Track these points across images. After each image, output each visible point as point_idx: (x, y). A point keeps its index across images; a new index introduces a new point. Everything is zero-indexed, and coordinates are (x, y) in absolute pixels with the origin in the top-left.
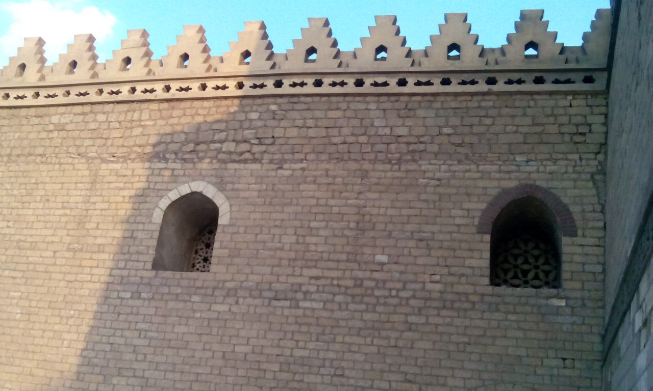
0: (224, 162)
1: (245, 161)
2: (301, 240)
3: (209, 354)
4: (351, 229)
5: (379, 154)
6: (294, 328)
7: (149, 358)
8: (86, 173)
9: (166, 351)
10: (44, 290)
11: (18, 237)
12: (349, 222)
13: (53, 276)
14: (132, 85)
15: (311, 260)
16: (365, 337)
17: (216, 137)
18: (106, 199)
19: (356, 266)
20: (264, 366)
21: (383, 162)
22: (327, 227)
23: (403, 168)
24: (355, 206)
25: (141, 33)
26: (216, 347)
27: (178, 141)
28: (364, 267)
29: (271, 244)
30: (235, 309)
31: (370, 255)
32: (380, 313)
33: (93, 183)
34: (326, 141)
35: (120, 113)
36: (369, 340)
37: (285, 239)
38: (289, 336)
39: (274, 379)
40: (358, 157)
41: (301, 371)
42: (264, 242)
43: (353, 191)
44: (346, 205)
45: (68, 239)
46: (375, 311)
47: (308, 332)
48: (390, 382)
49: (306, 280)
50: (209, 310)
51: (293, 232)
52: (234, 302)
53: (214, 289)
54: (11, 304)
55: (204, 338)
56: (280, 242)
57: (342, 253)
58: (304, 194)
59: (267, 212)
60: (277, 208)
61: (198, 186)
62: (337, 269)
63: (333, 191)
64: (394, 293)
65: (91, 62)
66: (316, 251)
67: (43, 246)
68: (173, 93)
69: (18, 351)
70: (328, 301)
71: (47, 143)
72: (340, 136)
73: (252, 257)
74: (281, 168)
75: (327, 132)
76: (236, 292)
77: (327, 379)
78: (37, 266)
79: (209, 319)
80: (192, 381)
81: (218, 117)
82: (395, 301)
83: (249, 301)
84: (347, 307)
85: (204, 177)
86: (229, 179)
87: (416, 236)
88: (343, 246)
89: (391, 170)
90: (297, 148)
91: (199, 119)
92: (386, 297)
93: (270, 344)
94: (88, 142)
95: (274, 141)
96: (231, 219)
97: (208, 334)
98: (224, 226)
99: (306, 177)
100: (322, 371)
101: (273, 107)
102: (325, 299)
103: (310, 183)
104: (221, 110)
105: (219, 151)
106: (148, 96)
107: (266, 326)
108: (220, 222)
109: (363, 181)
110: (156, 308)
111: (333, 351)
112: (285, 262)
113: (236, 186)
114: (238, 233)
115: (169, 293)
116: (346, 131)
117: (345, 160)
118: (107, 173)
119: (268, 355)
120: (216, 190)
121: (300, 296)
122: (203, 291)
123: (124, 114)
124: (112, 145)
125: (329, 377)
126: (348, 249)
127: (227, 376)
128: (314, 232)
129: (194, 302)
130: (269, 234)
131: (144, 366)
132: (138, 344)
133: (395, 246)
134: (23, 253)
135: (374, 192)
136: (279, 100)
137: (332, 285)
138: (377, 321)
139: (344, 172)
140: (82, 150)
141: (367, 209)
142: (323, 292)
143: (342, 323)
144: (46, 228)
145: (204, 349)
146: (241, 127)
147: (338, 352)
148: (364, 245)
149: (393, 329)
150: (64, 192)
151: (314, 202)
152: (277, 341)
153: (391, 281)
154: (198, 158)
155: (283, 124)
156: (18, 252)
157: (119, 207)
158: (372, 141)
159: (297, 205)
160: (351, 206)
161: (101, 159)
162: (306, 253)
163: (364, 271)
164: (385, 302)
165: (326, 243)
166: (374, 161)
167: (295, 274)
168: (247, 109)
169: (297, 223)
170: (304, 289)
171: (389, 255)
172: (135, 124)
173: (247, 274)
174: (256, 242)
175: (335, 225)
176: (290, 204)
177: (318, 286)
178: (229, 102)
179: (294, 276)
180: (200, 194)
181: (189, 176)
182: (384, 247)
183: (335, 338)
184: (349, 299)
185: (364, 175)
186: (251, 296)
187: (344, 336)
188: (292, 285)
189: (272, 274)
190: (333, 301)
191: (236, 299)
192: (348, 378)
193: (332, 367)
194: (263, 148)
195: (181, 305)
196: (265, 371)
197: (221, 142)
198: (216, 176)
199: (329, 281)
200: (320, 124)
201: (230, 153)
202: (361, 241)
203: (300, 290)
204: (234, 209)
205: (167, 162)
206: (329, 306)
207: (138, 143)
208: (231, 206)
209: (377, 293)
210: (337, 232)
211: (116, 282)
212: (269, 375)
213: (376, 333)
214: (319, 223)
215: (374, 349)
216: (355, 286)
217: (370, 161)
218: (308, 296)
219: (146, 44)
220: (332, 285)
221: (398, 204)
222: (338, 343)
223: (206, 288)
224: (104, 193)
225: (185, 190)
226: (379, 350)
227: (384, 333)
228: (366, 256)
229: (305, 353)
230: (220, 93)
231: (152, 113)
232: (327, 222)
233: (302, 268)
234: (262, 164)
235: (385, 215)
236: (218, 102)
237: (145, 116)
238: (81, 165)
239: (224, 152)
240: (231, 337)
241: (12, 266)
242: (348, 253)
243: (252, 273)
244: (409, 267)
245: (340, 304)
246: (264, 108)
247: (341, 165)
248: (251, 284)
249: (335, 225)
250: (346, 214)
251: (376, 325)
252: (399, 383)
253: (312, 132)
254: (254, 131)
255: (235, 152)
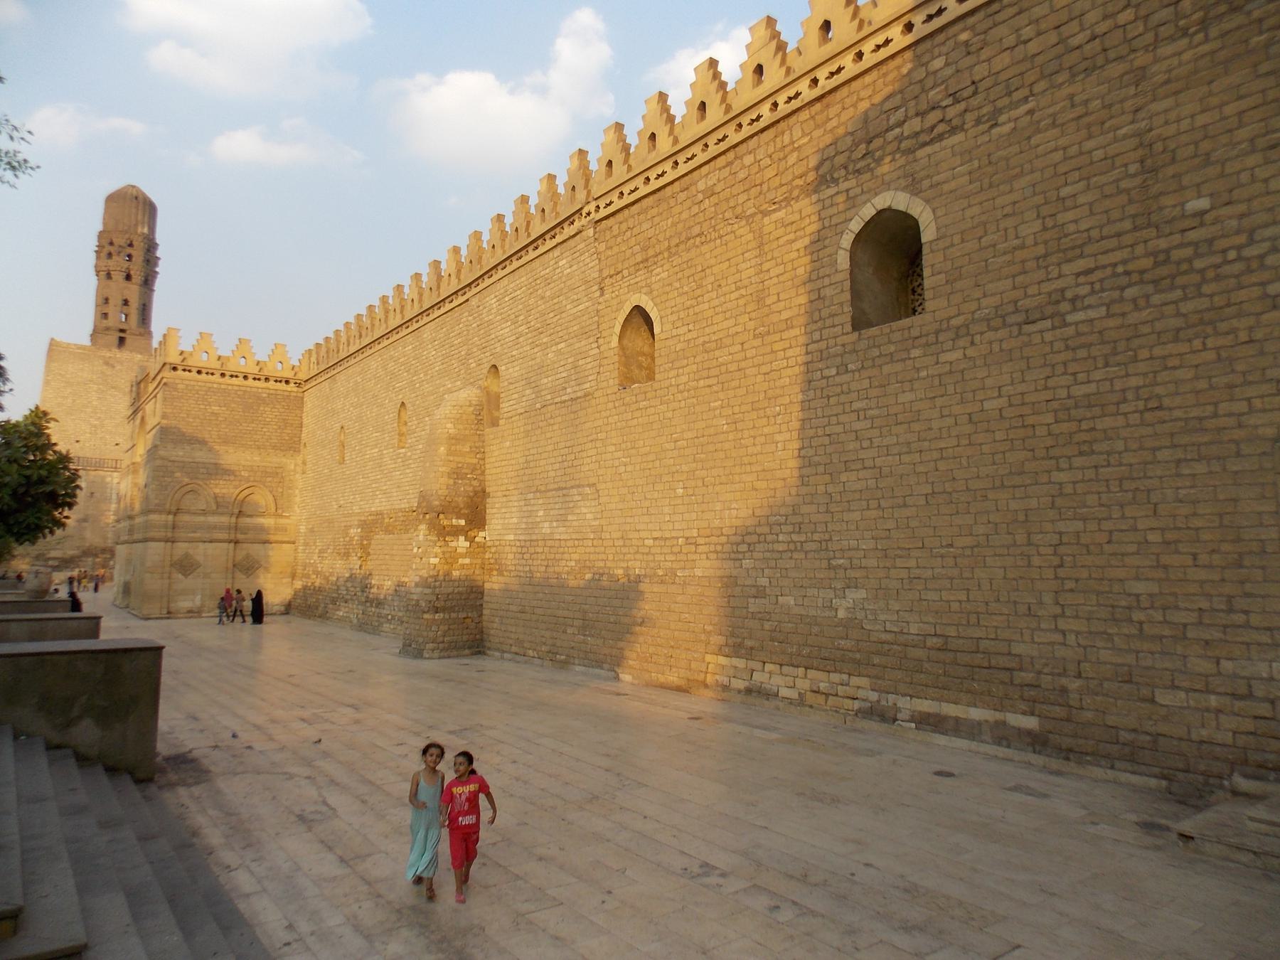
0: (911, 151)
1: (940, 137)
2: (1049, 222)
3: (950, 421)
4: (1134, 176)
5: (1162, 29)
6: (1069, 355)
7: (876, 442)
8: (750, 236)
9: (895, 429)
10: (742, 391)
11: (701, 340)
12: (1126, 165)
13: (748, 372)
14: (771, 101)
15: (1073, 248)
16: (1190, 340)
17: (892, 121)
18: (779, 260)
19: (1152, 232)
20: (1030, 420)
21: (1172, 39)
22: (1088, 188)
23: (1214, 31)
24: (1132, 136)
25: (764, 25)
26: (957, 409)
27: (844, 149)
28: (1167, 231)
29: (1004, 245)
30: (971, 352)
31: (1174, 206)
32: (1211, 296)
33: (761, 246)
34: (1060, 48)
35: (767, 144)
36: (1197, 344)
37: (1025, 230)
38: (1060, 369)
39: (1049, 434)
40: (1123, 50)
41: (1089, 415)
42: (994, 246)
43: (1123, 113)
44: (1116, 140)
45: (751, 325)
46: (1201, 295)
47: (1089, 357)
48: (1249, 400)
49: (1070, 281)
50: (937, 363)
51: (1035, 215)
52: (968, 345)
53: (937, 333)
54: (715, 417)
55: (939, 402)
56: (1017, 237)
57: (1122, 220)
58: (1040, 150)
59: (989, 200)
60: (1001, 187)
61: (884, 200)
62: (1121, 248)
63: (1089, 126)
64: (1232, 255)
65: (721, 94)
66: (1079, 232)
67: (728, 341)
68: (825, 85)
69: (735, 466)
70: (1113, 302)
71: (701, 218)
72: (1082, 30)
73: (980, 274)
74: (996, 125)
75: (1059, 34)
76: (968, 329)
77: (1134, 418)
78: (729, 366)
79: (940, 375)
80: (936, 461)
81: (889, 89)
82: (1238, 267)
83: (990, 335)
84: (1148, 302)
85: (889, 184)
86: (923, 174)
87: (1261, 143)
88: (1123, 207)
89: (1190, 47)
90: (1015, 82)
91: (864, 105)
92: (1217, 266)
93: (1032, 388)
94: (742, 198)
95: (977, 89)
96: (938, 229)
97: (942, 396)
98: (931, 242)
99: (1038, 122)
100: (1124, 408)
101: (964, 36)
102: (1107, 301)
103: (1046, 130)
104: (890, 77)
105: (900, 139)
106: (795, 104)
107: (1023, 364)
108: (923, 240)
109: (1140, 88)
110: (870, 378)
111: (1137, 374)
112: (1031, 265)
113: (936, 179)
114: (952, 245)
115: (881, 355)
116: (1091, 17)
117: (1100, 67)
118: (772, 227)
119: (1033, 404)
120: (909, 195)
121: (1065, 307)
122: (923, 340)
123: (772, 144)
124: (769, 190)
125: (1137, 415)
126: (1131, 210)
127: (981, 444)
128: (1069, 203)
129: (915, 358)
130: (998, 231)
131: (872, 453)
132: (858, 428)
133: (1222, 175)
134: (711, 355)
135: (1166, 97)
136: (971, 21)
137: (1115, 275)
138: (1208, 310)
139: (1102, 87)
140: (739, 210)
141: (1153, 133)
142: (1103, 290)
143: (1145, 329)
144: (726, 319)
145: (942, 416)
146: (923, 90)
147: (1145, 374)
148: (1161, 194)
149: (1239, 315)
150: (733, 270)
151: (1058, 156)
152: (1043, 382)
153: (1223, 236)
154: (875, 160)
155: (985, 54)
156: (706, 355)
157: (795, 266)
158: (1142, 12)
159: (1032, 172)
160: (1125, 137)
161: (761, 212)
162: (1063, 240)
163: (1167, 236)
164: (1218, 276)
165: (1092, 213)
166: (1157, 42)
167: (1050, 277)
168: (925, 59)
169: (1039, 199)
170: (1069, 294)
171: (1211, 195)
172: (788, 150)
173: (979, 299)
174: (981, 249)
175: (1103, 179)
176: (1021, 174)
177: (1092, 283)
178: (898, 61)
179: (1048, 280)
180: (889, 209)
181: (869, 191)
182: (1198, 185)
183: (1136, 356)
184: (1150, 288)
185: (1140, 75)
186: (990, 328)
187: (1152, 347)
188: (1050, 294)
189: (1014, 288)
190: (1122, 299)
191: (969, 338)
192: (1170, 409)
193: (1138, 399)
194: (962, 106)
195: (898, 367)
196: (1034, 426)
197: (900, 124)
198: (905, 177)
199: (1109, 271)
200: (1043, 26)
201: (917, 134)
202: (1154, 190)
203: (1064, 299)
204: (939, 213)
205: (837, 185)
206: (1116, 309)
207: (796, 174)
208: (934, 211)
209: (1199, 264)
210: (1109, 190)
211: (815, 359)
212: (1041, 431)
213: (1209, 330)
214: (1076, 186)
215: (1210, 356)
216: (1157, 264)
217: (1146, 48)
218: (1079, 304)
219: (776, 35)
220: (1115, 275)
221: (1215, 101)
222: (1142, 360)
223: (927, 335)
224: (776, 255)
225: (868, 212)
226: (1219, 355)
227: (1223, 326)
228: (1166, 212)
229: (1092, 388)
230: (884, 53)
231: (804, 126)
232: (1088, 178)
233: (1059, 265)
234: (966, 131)
235: (1193, 129)
236: (884, 69)
237: (797, 132)
238: (742, 229)
239: (908, 138)
240: (974, 391)
241: (705, 374)
242: (1134, 216)
243: (985, 296)
244: (1255, 203)
245: (1134, 300)
246: (951, 43)
247: (1094, 77)
248: (987, 311)
249: (1103, 179)
250: (1118, 155)
251: (1207, 316)
252: (1266, 399)
253: (1033, 47)
254: (943, 87)
255: (922, 131)
